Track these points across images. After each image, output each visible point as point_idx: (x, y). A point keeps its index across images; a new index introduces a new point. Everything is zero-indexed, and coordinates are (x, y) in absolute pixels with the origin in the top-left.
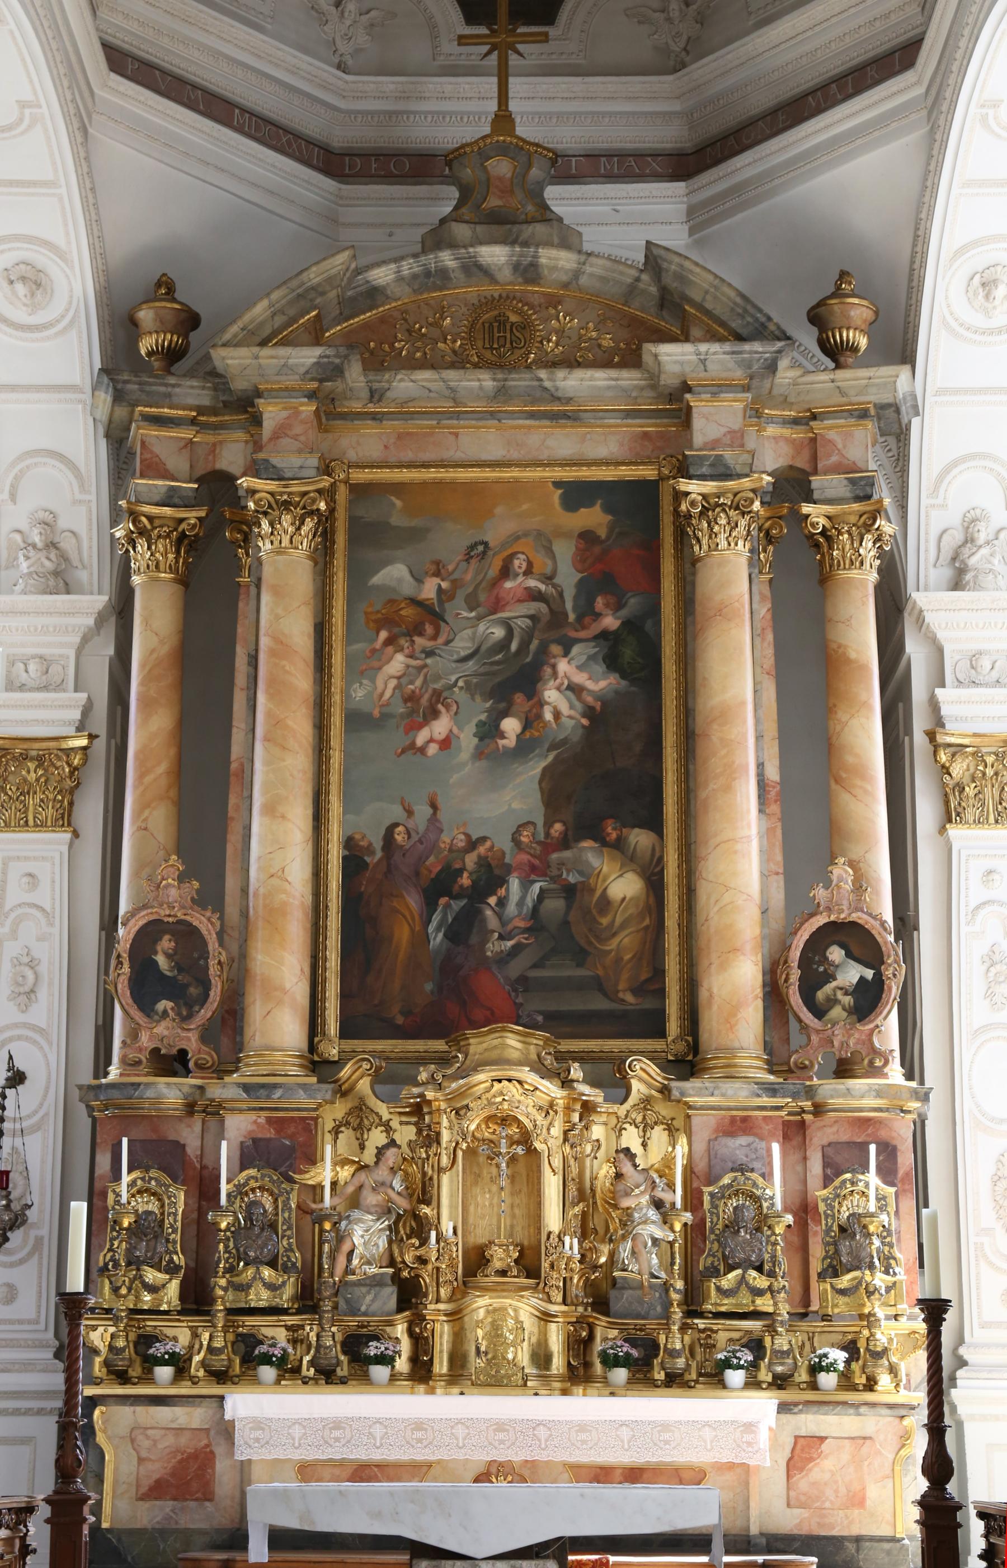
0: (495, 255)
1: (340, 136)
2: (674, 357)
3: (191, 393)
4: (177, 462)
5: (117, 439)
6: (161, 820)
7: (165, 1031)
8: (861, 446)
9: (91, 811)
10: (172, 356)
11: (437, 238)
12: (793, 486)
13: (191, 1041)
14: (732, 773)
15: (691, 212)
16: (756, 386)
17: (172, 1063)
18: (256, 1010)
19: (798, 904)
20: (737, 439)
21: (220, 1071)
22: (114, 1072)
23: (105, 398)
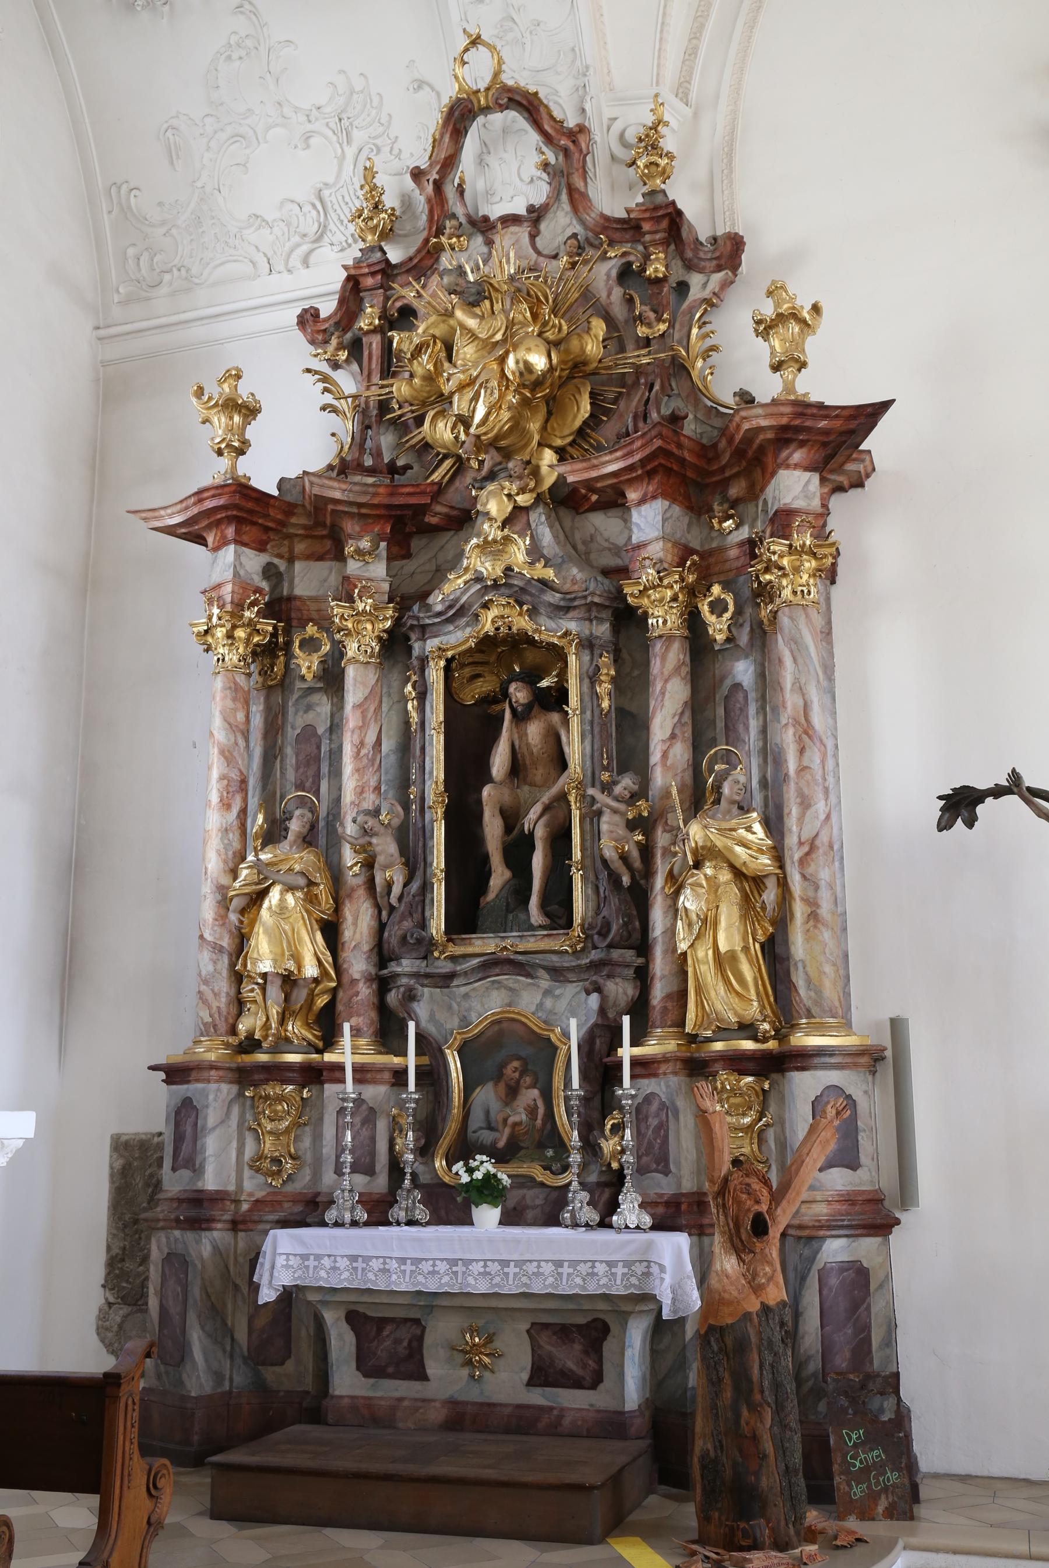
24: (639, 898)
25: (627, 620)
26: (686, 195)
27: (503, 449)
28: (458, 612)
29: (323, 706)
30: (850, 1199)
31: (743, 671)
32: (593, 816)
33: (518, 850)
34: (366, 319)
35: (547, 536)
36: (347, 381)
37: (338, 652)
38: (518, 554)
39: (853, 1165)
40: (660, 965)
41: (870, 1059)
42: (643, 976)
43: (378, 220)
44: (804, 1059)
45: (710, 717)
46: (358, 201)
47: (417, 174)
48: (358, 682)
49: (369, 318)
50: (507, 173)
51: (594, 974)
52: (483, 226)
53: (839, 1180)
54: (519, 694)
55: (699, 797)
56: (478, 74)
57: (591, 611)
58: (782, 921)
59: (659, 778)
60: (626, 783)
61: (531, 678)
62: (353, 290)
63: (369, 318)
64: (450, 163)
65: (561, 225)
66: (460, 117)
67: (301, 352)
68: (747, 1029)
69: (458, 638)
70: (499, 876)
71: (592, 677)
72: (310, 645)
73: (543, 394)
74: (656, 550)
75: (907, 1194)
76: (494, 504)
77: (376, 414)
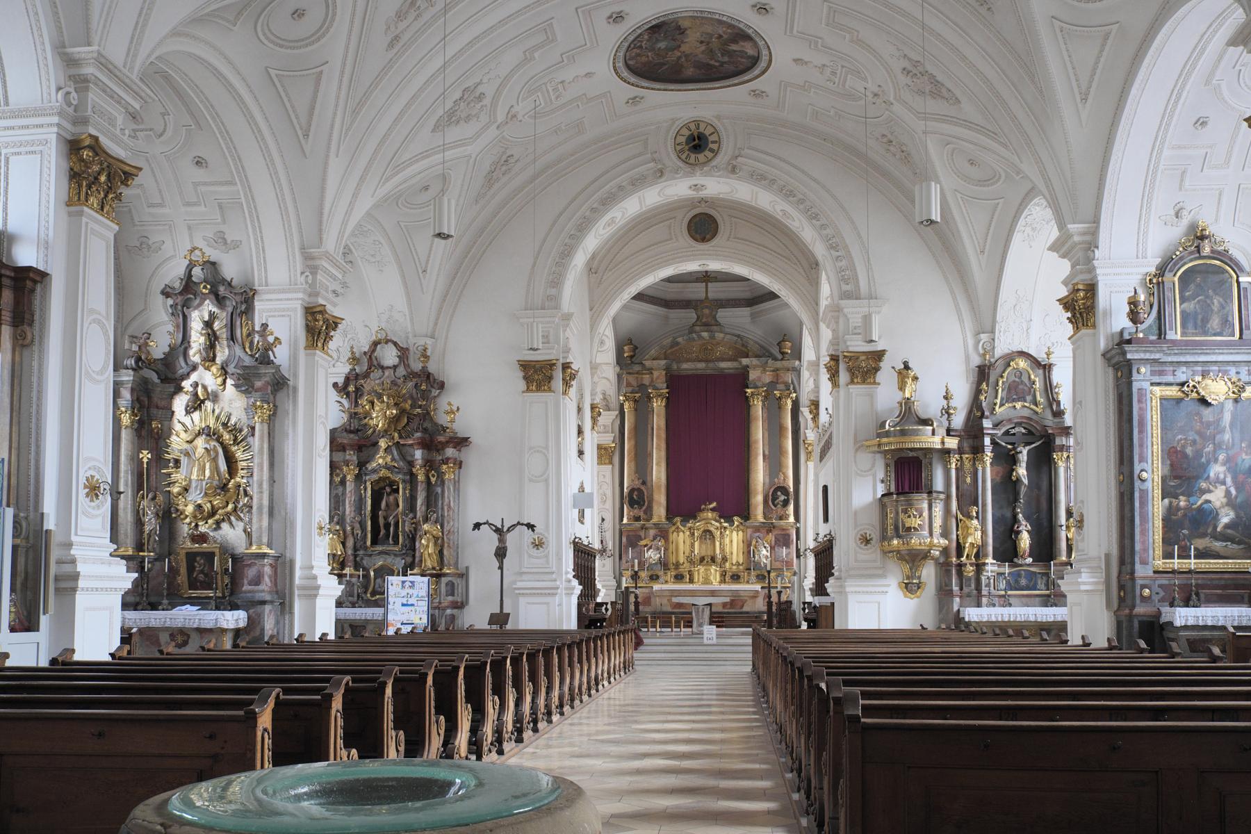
0: (705, 334)
1: (669, 297)
2: (745, 361)
3: (637, 368)
4: (635, 384)
5: (619, 376)
6: (633, 464)
7: (636, 512)
8: (789, 377)
9: (616, 459)
10: (632, 357)
11: (691, 330)
12: (772, 385)
13: (642, 514)
14: (757, 455)
15: (752, 315)
16: (764, 367)
17: (637, 519)
18: (655, 507)
19: (772, 483)
20: (759, 379)
21: (648, 520)
22: (625, 521)
23: (618, 369)
24: (413, 540)
25: (413, 476)
26: (432, 368)
27: (385, 433)
28: (374, 471)
29: (341, 489)
30: (452, 602)
31: (439, 490)
32: (404, 522)
33: (387, 526)
34: (350, 388)
35: (395, 453)
36: (345, 403)
37: (345, 477)
38: (389, 459)
39: (453, 594)
40: (417, 554)
41: (461, 576)
42: (414, 556)
43: (354, 359)
44: (445, 575)
45: (431, 502)
46: (349, 355)
47: (365, 353)
48: (350, 486)
49: (351, 388)
50: (389, 356)
51: (403, 556)
52: (383, 368)
53: (450, 598)
54: (388, 489)
55: (426, 520)
56: (381, 336)
57: (405, 474)
58: (442, 546)
59: (419, 514)
60: (411, 515)
61: (391, 486)
62: (347, 379)
63: (351, 388)
64: (374, 351)
65: (401, 371)
66: (375, 344)
67: (334, 395)
68: (434, 568)
69: (375, 477)
70: (383, 532)
71: (404, 489)
72: (338, 475)
73: (395, 420)
74: (420, 462)
75: (467, 603)
76: (383, 443)
77: (353, 416)
